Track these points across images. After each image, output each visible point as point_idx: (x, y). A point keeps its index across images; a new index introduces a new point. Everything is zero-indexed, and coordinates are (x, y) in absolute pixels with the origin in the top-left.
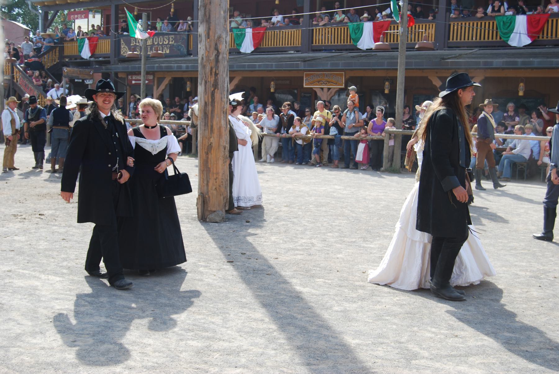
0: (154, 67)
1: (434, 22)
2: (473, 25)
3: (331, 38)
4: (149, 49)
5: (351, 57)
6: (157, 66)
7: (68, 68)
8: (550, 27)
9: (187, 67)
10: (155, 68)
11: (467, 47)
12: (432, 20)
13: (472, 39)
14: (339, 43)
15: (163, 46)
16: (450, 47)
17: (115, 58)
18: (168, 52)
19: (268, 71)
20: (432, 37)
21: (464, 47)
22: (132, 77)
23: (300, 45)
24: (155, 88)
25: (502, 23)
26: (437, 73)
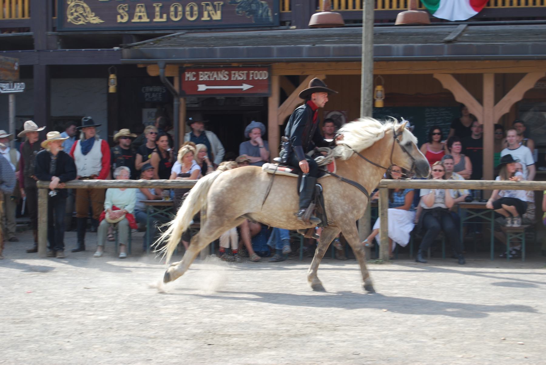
0: (269, 51)
4: (158, 9)
6: (310, 48)
10: (275, 53)
17: (47, 30)
18: (217, 16)
22: (197, 76)
24: (273, 101)
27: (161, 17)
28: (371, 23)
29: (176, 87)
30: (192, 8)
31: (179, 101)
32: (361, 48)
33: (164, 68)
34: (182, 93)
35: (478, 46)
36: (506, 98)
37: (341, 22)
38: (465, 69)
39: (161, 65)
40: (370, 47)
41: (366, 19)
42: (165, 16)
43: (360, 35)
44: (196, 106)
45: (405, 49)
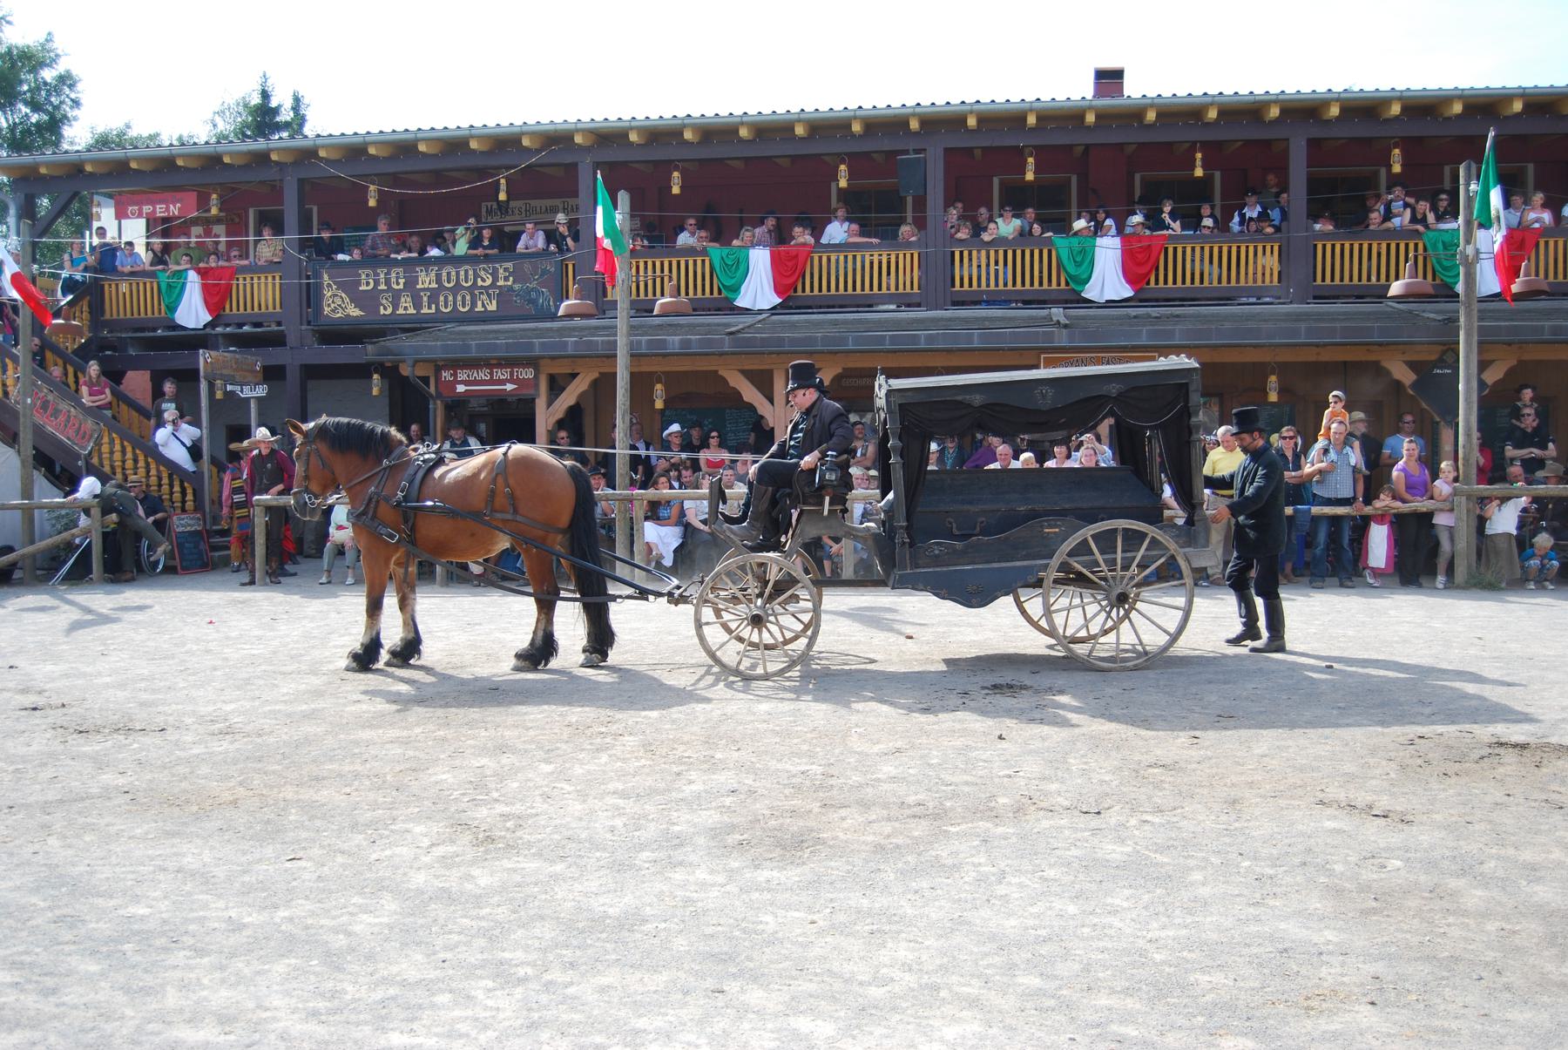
1: (1274, 241)
2: (846, 262)
4: (425, 299)
5: (1135, 317)
7: (212, 353)
8: (1542, 257)
9: (686, 344)
11: (1358, 297)
13: (1369, 279)
14: (1045, 286)
15: (476, 292)
18: (493, 307)
20: (1272, 274)
23: (916, 290)
24: (541, 404)
25: (1440, 246)
26: (1404, 353)
27: (430, 308)
28: (625, 314)
29: (432, 390)
30: (464, 297)
31: (435, 404)
33: (414, 366)
34: (439, 395)
35: (762, 338)
37: (594, 311)
38: (754, 365)
39: (410, 362)
40: (625, 339)
42: (433, 306)
43: (616, 327)
44: (485, 409)
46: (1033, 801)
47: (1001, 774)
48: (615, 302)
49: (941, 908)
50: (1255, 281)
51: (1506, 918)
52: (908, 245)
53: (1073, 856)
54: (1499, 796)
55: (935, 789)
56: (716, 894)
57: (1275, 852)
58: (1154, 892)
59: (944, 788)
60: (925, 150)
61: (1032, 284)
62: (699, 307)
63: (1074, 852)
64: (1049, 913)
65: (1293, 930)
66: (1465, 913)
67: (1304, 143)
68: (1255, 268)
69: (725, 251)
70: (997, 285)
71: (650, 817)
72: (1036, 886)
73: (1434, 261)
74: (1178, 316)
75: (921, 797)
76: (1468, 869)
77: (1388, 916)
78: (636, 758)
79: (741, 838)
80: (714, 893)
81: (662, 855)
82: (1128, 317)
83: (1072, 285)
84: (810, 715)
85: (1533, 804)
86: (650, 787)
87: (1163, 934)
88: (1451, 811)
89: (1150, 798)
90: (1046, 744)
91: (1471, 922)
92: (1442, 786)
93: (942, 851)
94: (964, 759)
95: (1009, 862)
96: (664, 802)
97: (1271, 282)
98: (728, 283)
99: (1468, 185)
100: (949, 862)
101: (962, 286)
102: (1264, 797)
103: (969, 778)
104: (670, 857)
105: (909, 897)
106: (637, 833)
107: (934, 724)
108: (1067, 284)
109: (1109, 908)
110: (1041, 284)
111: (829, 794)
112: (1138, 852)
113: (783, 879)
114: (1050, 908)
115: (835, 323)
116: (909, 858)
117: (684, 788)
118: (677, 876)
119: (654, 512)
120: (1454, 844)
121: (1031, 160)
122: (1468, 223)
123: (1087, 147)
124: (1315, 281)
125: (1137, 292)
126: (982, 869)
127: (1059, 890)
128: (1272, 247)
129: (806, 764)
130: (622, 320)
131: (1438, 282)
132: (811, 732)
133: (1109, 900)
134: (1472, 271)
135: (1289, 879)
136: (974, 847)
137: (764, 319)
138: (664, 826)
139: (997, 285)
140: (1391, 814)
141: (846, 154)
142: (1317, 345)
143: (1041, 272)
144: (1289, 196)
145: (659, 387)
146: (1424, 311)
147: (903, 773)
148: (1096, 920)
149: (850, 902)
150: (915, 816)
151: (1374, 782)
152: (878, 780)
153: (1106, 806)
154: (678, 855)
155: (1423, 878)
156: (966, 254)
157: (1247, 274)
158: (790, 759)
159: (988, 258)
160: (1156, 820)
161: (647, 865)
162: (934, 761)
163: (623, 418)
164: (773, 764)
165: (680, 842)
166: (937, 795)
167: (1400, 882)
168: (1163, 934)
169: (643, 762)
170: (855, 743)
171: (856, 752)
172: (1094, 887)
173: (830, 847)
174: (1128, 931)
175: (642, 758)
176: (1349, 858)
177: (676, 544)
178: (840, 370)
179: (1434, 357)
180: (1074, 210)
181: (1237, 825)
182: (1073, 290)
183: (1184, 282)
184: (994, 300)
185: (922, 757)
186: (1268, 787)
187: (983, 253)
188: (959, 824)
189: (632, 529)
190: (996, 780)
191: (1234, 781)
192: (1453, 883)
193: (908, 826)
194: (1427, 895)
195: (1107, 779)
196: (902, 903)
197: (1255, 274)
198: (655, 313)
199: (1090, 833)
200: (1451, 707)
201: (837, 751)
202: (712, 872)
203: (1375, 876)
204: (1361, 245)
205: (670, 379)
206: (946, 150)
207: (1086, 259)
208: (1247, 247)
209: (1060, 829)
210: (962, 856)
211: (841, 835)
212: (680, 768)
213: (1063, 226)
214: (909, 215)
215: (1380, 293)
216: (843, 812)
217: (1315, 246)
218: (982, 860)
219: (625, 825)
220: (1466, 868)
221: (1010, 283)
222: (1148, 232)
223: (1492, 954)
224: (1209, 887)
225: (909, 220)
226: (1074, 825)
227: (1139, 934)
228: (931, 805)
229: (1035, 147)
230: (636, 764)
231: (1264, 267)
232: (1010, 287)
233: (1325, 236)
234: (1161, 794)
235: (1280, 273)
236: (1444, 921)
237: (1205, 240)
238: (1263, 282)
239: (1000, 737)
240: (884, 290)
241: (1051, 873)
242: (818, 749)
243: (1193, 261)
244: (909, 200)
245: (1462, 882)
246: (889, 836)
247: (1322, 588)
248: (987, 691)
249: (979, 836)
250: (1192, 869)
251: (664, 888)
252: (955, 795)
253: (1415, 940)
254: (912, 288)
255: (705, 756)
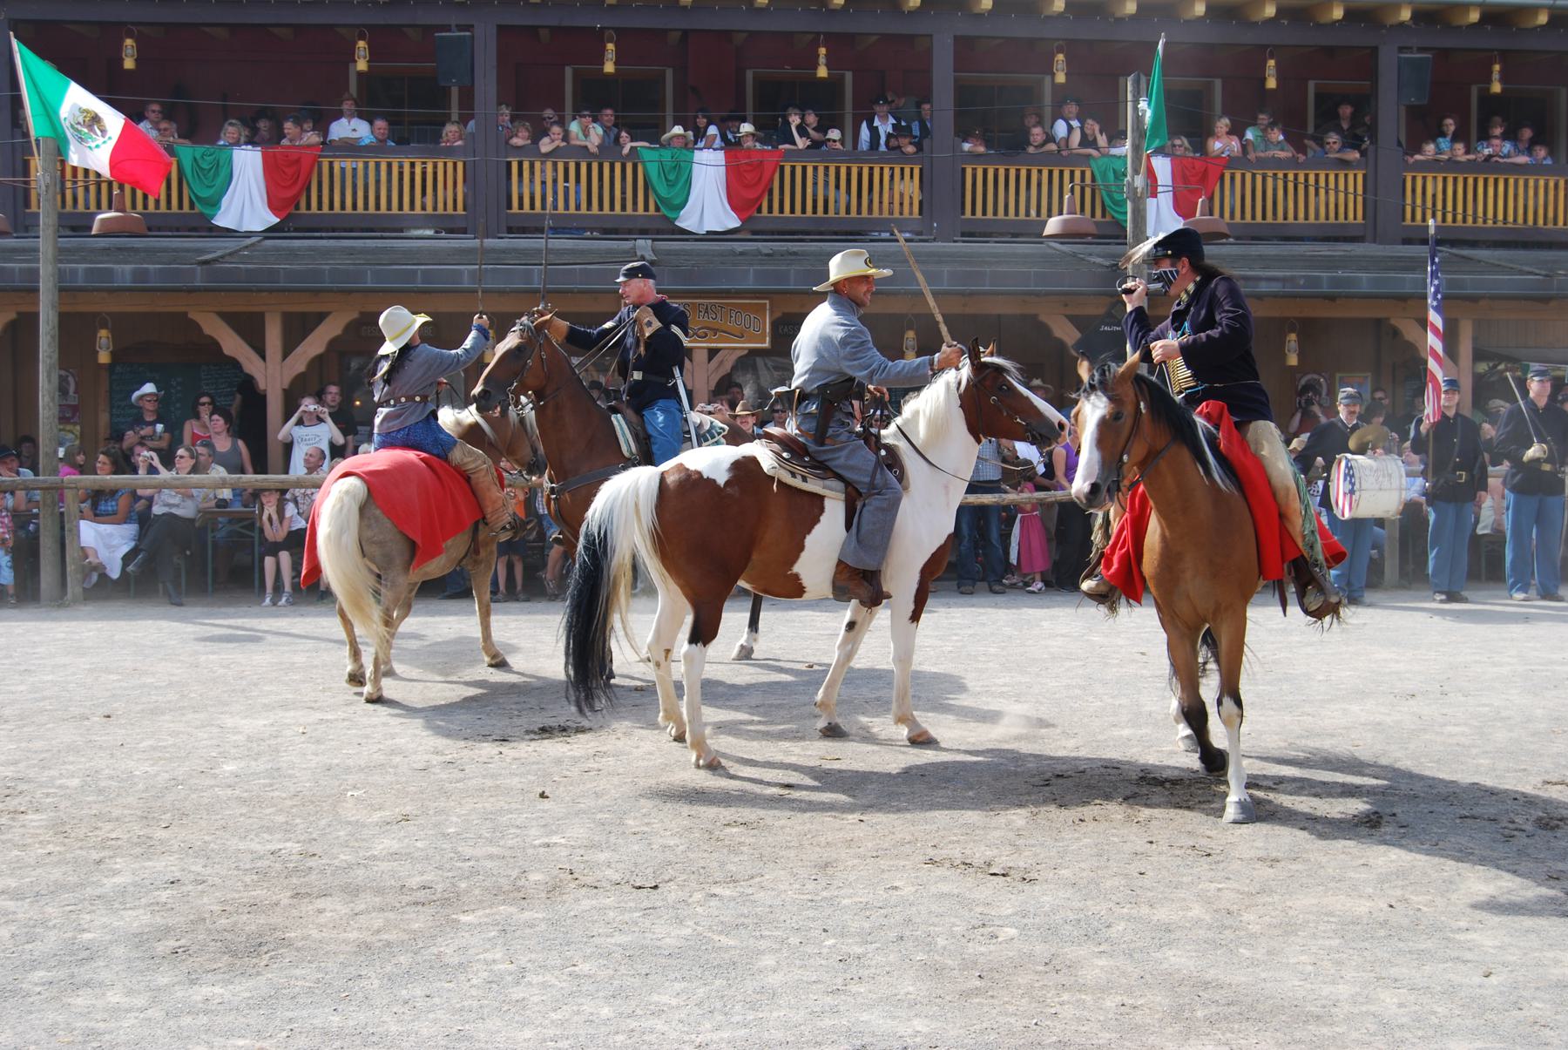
3: (577, 193)
5: (742, 254)
9: (140, 275)
12: (915, 153)
13: (1028, 214)
16: (969, 234)
19: (502, 292)
20: (911, 204)
21: (1002, 235)
23: (460, 211)
25: (1111, 176)
28: (50, 231)
32: (38, 269)
36: (299, 349)
38: (239, 305)
40: (50, 268)
41: (44, 224)
43: (36, 250)
45: (134, 272)
46: (575, 876)
47: (537, 842)
48: (37, 215)
49: (435, 1021)
50: (891, 213)
51: (1129, 991)
52: (450, 152)
53: (616, 945)
54: (1140, 844)
55: (448, 866)
56: (133, 1021)
57: (867, 925)
58: (713, 983)
59: (459, 864)
60: (472, 26)
61: (612, 208)
62: (155, 225)
63: (619, 939)
64: (576, 1018)
65: (876, 1021)
66: (1082, 988)
67: (950, 41)
68: (891, 197)
69: (200, 150)
70: (567, 207)
71: (51, 924)
72: (564, 985)
73: (1104, 193)
74: (795, 254)
75: (428, 877)
76: (1091, 935)
77: (992, 997)
78: (41, 842)
79: (178, 944)
80: (129, 1021)
81: (62, 973)
82: (733, 253)
83: (664, 211)
84: (290, 776)
85: (1178, 852)
86: (56, 882)
87: (716, 1036)
88: (1083, 865)
89: (722, 864)
90: (600, 801)
91: (1088, 998)
92: (1076, 835)
93: (447, 948)
94: (490, 825)
95: (533, 956)
96: (73, 901)
97: (911, 213)
98: (205, 193)
99: (1136, 102)
100: (455, 960)
101: (521, 206)
102: (863, 857)
103: (494, 850)
104: (72, 976)
105: (395, 1010)
106: (29, 946)
107: (458, 781)
108: (657, 209)
109: (652, 1007)
110: (624, 208)
111: (307, 879)
112: (698, 935)
113: (227, 996)
114: (578, 1013)
115: (351, 252)
116: (402, 959)
117: (105, 881)
118: (79, 1001)
119: (99, 504)
120: (1080, 905)
121: (610, 46)
122: (1137, 149)
123: (685, 33)
124: (963, 213)
125: (744, 221)
126: (496, 967)
127: (592, 988)
128: (912, 169)
129: (279, 840)
130: (46, 242)
131: (1108, 219)
132: (291, 798)
133: (655, 998)
134: (1141, 207)
135: (880, 958)
136: (489, 940)
137: (253, 245)
138: (69, 935)
139: (567, 207)
140: (1012, 872)
141: (365, 26)
142: (962, 294)
143: (623, 192)
144: (932, 106)
145: (103, 333)
146: (1090, 255)
147: (408, 846)
148: (633, 1024)
149: (315, 1021)
150: (416, 903)
151: (997, 834)
152: (375, 858)
153: (667, 878)
154: (84, 973)
155: (1039, 948)
156: (526, 165)
157: (881, 202)
158: (257, 835)
159: (555, 170)
160: (728, 892)
161: (38, 989)
162: (451, 830)
163: (49, 376)
164: (234, 843)
165: (89, 954)
166: (450, 874)
167: (1011, 954)
168: (716, 1036)
169: (50, 848)
170: (350, 812)
171: (349, 823)
172: (637, 981)
173: (298, 950)
174: (674, 1035)
175: (49, 842)
176: (955, 929)
177: (125, 549)
178: (355, 315)
179: (1101, 311)
180: (669, 114)
181: (825, 894)
182: (665, 217)
183: (804, 211)
184: (563, 227)
185: (435, 826)
186: (870, 845)
187: (549, 165)
188: (473, 911)
189: (62, 528)
190: (530, 851)
191: (830, 839)
192: (1072, 952)
193: (407, 916)
194: (1041, 968)
195: (672, 843)
196: (385, 1018)
197: (891, 203)
198: (93, 233)
199: (641, 913)
200: (1100, 737)
201: (323, 822)
202: (130, 992)
203: (983, 949)
204: (1018, 171)
205: (119, 323)
206: (503, 30)
207: (681, 179)
208: (882, 169)
209: (602, 910)
210: (472, 951)
211: (315, 933)
212: (102, 855)
213: (651, 131)
214: (455, 112)
215: (1034, 231)
216: (320, 903)
217: (964, 170)
218: (498, 956)
219: (13, 936)
220: (1091, 933)
221: (584, 205)
222: (758, 146)
223: (1108, 1036)
224: (782, 974)
225: (455, 117)
226: (623, 904)
227: (686, 1038)
228: (440, 887)
229: (616, 30)
230: (40, 851)
231: (902, 195)
232: (584, 210)
233: (974, 157)
234: (736, 860)
235: (921, 203)
236: (1057, 1000)
237: (834, 156)
238: (901, 213)
239: (543, 795)
240: (418, 210)
241: (584, 968)
242: (298, 821)
243: (815, 184)
244: (455, 91)
245: (1082, 952)
246: (378, 931)
247: (972, 593)
248: (532, 736)
249: (498, 924)
250: (762, 952)
251: (60, 1019)
252: (474, 872)
253: (1018, 1024)
254: (455, 208)
255: (139, 837)
